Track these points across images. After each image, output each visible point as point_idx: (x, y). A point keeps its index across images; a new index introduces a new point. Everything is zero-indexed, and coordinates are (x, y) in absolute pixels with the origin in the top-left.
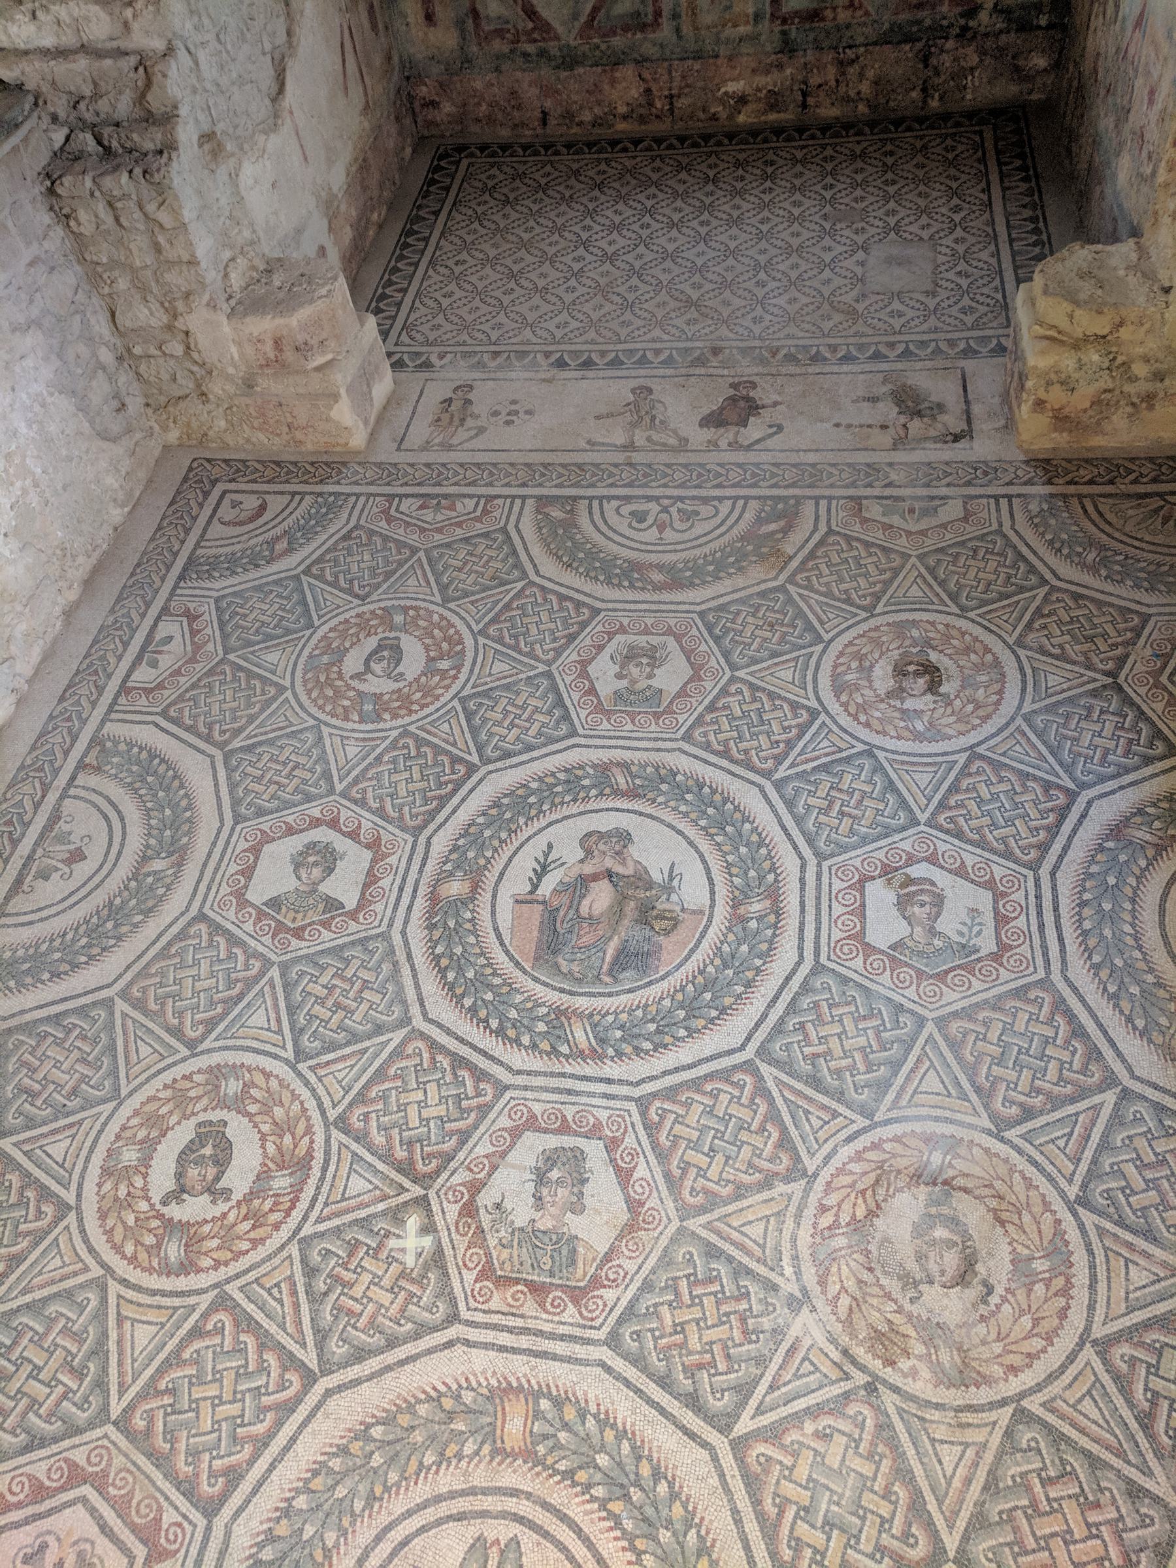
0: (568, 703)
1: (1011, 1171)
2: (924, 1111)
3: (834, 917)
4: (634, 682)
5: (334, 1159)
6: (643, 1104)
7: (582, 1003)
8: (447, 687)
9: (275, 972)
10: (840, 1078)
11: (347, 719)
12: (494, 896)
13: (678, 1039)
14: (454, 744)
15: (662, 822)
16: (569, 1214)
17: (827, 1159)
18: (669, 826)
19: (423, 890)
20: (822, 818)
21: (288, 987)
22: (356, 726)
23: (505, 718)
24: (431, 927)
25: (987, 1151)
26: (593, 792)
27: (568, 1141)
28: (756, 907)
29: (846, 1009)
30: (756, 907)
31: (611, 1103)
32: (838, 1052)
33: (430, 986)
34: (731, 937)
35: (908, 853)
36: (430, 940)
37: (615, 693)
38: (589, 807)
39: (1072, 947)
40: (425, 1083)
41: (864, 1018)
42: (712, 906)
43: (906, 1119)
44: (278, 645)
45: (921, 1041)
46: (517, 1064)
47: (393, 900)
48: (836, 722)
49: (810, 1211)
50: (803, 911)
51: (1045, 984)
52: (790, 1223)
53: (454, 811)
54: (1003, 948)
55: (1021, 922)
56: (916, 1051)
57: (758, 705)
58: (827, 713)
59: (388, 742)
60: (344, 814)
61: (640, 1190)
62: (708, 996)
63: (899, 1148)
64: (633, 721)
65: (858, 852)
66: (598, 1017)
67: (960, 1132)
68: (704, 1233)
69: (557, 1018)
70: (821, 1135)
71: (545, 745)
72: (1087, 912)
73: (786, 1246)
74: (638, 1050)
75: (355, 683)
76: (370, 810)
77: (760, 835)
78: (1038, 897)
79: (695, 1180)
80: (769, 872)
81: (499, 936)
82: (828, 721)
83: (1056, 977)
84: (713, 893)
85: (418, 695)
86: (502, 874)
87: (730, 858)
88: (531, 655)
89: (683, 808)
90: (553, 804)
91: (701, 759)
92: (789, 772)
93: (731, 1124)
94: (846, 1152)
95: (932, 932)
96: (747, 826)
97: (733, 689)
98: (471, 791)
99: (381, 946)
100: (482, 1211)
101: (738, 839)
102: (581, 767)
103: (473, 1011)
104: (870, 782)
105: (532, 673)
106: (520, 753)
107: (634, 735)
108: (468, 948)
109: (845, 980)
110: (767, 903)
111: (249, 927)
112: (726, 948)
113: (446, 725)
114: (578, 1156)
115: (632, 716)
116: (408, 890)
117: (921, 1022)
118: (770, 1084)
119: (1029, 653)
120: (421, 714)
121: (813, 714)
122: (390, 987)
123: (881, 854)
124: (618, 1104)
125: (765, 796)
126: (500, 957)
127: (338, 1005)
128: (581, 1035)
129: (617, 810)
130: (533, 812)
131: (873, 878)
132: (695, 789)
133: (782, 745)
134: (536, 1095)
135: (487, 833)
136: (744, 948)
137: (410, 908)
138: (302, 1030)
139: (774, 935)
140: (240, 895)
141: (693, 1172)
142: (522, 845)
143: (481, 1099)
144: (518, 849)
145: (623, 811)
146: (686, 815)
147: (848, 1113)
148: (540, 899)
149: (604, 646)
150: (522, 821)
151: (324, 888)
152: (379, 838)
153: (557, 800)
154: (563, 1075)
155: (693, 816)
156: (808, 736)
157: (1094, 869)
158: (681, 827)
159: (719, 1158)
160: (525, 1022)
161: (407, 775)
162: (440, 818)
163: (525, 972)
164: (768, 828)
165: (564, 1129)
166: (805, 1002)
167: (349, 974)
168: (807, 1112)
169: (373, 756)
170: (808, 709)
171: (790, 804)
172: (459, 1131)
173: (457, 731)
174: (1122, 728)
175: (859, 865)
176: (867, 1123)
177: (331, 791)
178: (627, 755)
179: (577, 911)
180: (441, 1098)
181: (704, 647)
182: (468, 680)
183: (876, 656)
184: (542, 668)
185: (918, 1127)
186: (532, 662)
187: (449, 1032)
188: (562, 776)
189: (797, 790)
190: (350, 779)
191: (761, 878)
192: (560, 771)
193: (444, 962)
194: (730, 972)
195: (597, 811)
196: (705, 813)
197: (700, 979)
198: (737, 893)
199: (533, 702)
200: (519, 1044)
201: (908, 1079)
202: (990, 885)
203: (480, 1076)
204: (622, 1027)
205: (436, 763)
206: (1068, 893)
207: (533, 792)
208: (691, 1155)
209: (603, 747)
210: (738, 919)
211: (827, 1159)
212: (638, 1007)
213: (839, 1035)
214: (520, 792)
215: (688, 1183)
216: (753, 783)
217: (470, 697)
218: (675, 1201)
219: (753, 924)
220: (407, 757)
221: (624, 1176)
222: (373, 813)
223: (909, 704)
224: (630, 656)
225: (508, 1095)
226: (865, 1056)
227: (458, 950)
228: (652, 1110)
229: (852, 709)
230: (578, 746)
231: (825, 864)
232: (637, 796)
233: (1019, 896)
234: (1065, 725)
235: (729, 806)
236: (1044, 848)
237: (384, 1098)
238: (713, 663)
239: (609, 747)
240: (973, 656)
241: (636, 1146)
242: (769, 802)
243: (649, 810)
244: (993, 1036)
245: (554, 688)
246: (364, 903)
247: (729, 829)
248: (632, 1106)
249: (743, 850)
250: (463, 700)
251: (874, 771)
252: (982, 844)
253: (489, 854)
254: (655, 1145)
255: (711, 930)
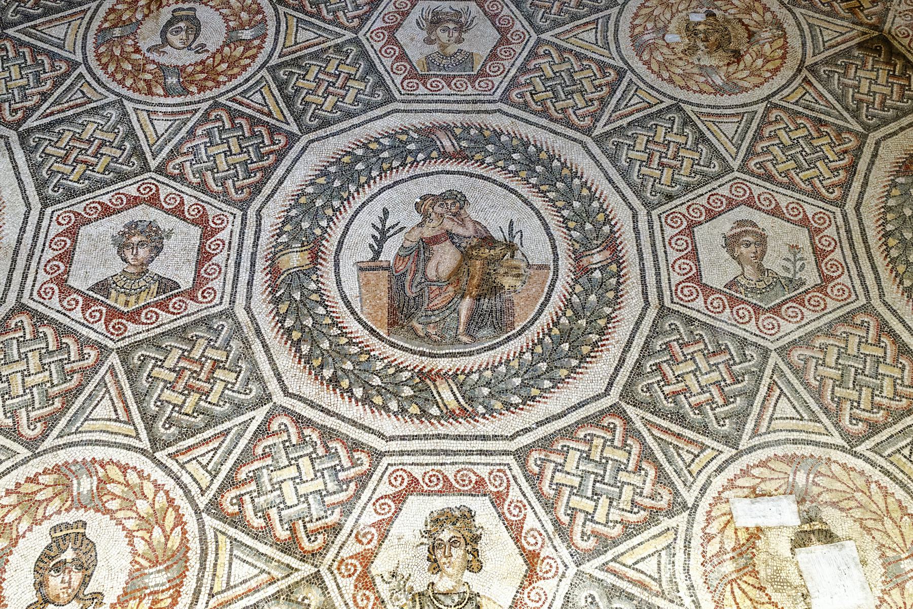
0: (381, 69)
1: (868, 483)
2: (782, 436)
3: (671, 262)
4: (443, 47)
5: (212, 547)
6: (521, 455)
7: (444, 364)
8: (253, 57)
9: (114, 359)
10: (701, 413)
11: (150, 92)
12: (337, 265)
13: (544, 390)
14: (270, 114)
15: (494, 182)
16: (467, 572)
17: (703, 490)
18: (501, 185)
19: (260, 264)
20: (644, 170)
21: (132, 374)
22: (162, 100)
23: (318, 86)
24: (277, 301)
25: (844, 466)
26: (421, 156)
27: (453, 502)
28: (597, 258)
29: (696, 348)
30: (597, 258)
31: (490, 459)
32: (695, 388)
33: (285, 360)
34: (578, 289)
35: (727, 198)
36: (278, 313)
37: (427, 58)
38: (418, 172)
39: (884, 274)
40: (296, 459)
41: (714, 354)
42: (556, 260)
43: (767, 445)
44: (63, 18)
45: (768, 372)
46: (389, 431)
47: (230, 275)
48: (642, 80)
49: (696, 542)
50: (641, 259)
51: (866, 309)
52: (680, 557)
53: (280, 183)
54: (826, 279)
55: (837, 255)
56: (766, 381)
57: (565, 66)
58: (633, 71)
59: (198, 115)
60: (163, 192)
61: (532, 541)
62: (566, 346)
63: (766, 473)
64: (449, 86)
65: (683, 199)
66: (462, 377)
67: (818, 452)
68: (600, 575)
69: (422, 381)
70: (695, 468)
71: (365, 111)
72: (892, 242)
73: (680, 577)
74: (508, 406)
75: (154, 56)
76: (190, 185)
77: (590, 189)
78: (848, 231)
79: (584, 524)
80: (604, 224)
81: (348, 304)
82: (634, 79)
83: (876, 302)
84: (554, 247)
85: (224, 66)
86: (341, 243)
87: (565, 213)
88: (335, 22)
89: (512, 167)
90: (382, 171)
91: (522, 119)
92: (607, 128)
93: (609, 467)
94: (719, 482)
95: (761, 270)
96: (576, 181)
97: (541, 51)
98: (296, 160)
99: (227, 324)
100: (378, 580)
101: (568, 195)
102: (405, 132)
103: (334, 381)
104: (682, 134)
105: (339, 41)
106: (340, 121)
107: (452, 98)
108: (318, 318)
109: (690, 321)
110: (607, 253)
111: (77, 314)
112: (575, 299)
113: (258, 96)
114: (468, 515)
115: (448, 80)
116: (246, 264)
117: (765, 354)
118: (639, 424)
119: (803, 11)
120: (230, 85)
121: (621, 74)
122: (243, 365)
123: (703, 201)
124: (497, 459)
125: (589, 152)
126: (353, 326)
127: (190, 388)
128: (447, 394)
129: (448, 173)
130: (363, 179)
131: (700, 223)
132: (521, 148)
133: (596, 103)
134: (412, 459)
135: (319, 203)
136: (593, 298)
137: (250, 283)
138: (155, 417)
139: (618, 283)
140: (62, 282)
141: (580, 517)
142: (357, 213)
143: (357, 469)
144: (354, 217)
145: (453, 173)
146: (516, 173)
147: (715, 444)
148: (385, 264)
149: (408, 13)
150: (352, 188)
151: (155, 268)
152: (205, 214)
153: (385, 166)
154: (438, 436)
155: (523, 174)
156: (618, 94)
157: (892, 202)
158: (512, 185)
159: (604, 501)
160: (390, 387)
161: (224, 147)
162: (267, 190)
163: (381, 339)
164: (596, 183)
165: (448, 489)
166: (658, 344)
167: (196, 354)
168: (676, 447)
169: (185, 130)
170: (614, 68)
171: (613, 159)
172: (341, 503)
173: (270, 101)
174: (894, 76)
175: (684, 211)
176: (734, 452)
177: (145, 168)
178: (449, 118)
179: (424, 273)
180: (315, 472)
181: (506, 11)
182: (274, 49)
183: (668, 16)
184: (349, 35)
185: (779, 451)
186: (338, 30)
187: (312, 405)
188: (386, 142)
189: (618, 145)
190: (164, 154)
191: (598, 229)
192: (384, 137)
193: (296, 335)
194: (583, 322)
195: (427, 175)
196: (535, 171)
197: (556, 331)
198: (577, 246)
199: (345, 69)
200: (388, 410)
201: (763, 407)
202: (804, 222)
203: (355, 446)
204: (488, 384)
205: (254, 135)
206: (873, 226)
207: (358, 159)
208: (576, 501)
209: (423, 111)
210: (582, 271)
211: (703, 490)
212: (500, 363)
213: (694, 372)
214: (346, 159)
215: (578, 529)
216: (575, 140)
217: (279, 66)
218: (569, 547)
219: (597, 275)
220: (222, 130)
221: (515, 530)
222: (194, 188)
223: (706, 61)
224: (436, 21)
225: (385, 461)
226: (721, 389)
227: (309, 322)
228: (531, 461)
229: (655, 67)
230: (397, 111)
231: (655, 213)
232: (466, 158)
233: (831, 231)
234: (845, 75)
235: (556, 163)
236: (846, 186)
237: (255, 477)
238: (518, 26)
239: (429, 111)
240: (754, 15)
241: (521, 498)
242: (593, 157)
243: (479, 171)
244: (831, 360)
245: (364, 54)
246: (199, 281)
247: (559, 185)
248: (510, 459)
249: (576, 204)
250: (273, 70)
251: (685, 124)
252: (791, 185)
253: (324, 223)
254: (540, 495)
255: (558, 282)
